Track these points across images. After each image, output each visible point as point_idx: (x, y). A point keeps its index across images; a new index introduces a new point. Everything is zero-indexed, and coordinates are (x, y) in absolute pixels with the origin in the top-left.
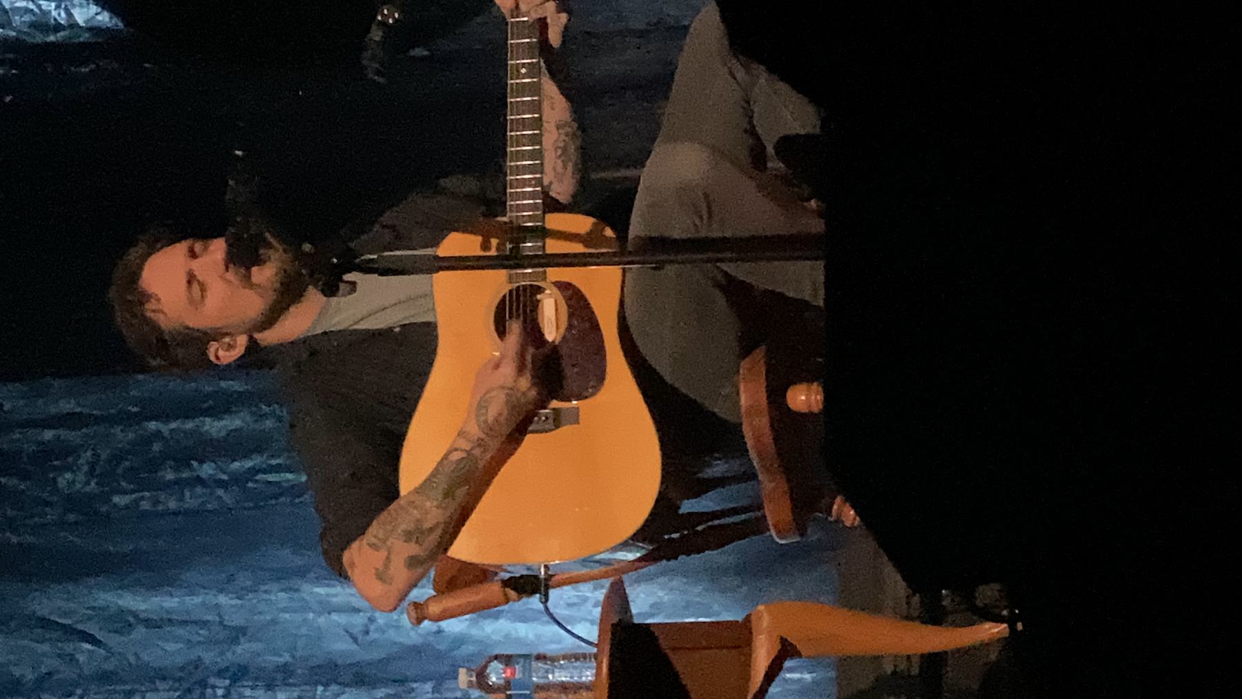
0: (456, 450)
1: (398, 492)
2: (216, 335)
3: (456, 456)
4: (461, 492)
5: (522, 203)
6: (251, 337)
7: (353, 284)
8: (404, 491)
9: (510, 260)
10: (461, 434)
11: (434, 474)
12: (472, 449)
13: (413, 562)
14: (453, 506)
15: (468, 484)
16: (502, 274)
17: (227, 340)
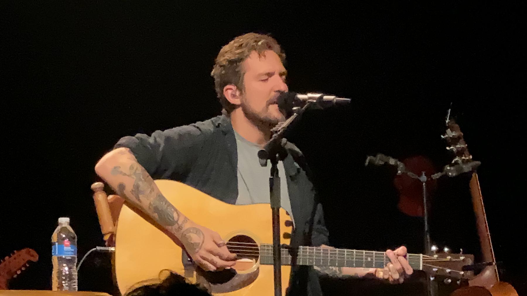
0: (178, 215)
1: (159, 178)
2: (241, 88)
3: (175, 215)
4: (156, 215)
5: (307, 255)
6: (239, 106)
7: (265, 165)
8: (159, 183)
9: (277, 247)
10: (186, 220)
11: (166, 202)
12: (178, 224)
13: (122, 187)
14: (150, 212)
15: (160, 219)
16: (271, 242)
17: (238, 93)
